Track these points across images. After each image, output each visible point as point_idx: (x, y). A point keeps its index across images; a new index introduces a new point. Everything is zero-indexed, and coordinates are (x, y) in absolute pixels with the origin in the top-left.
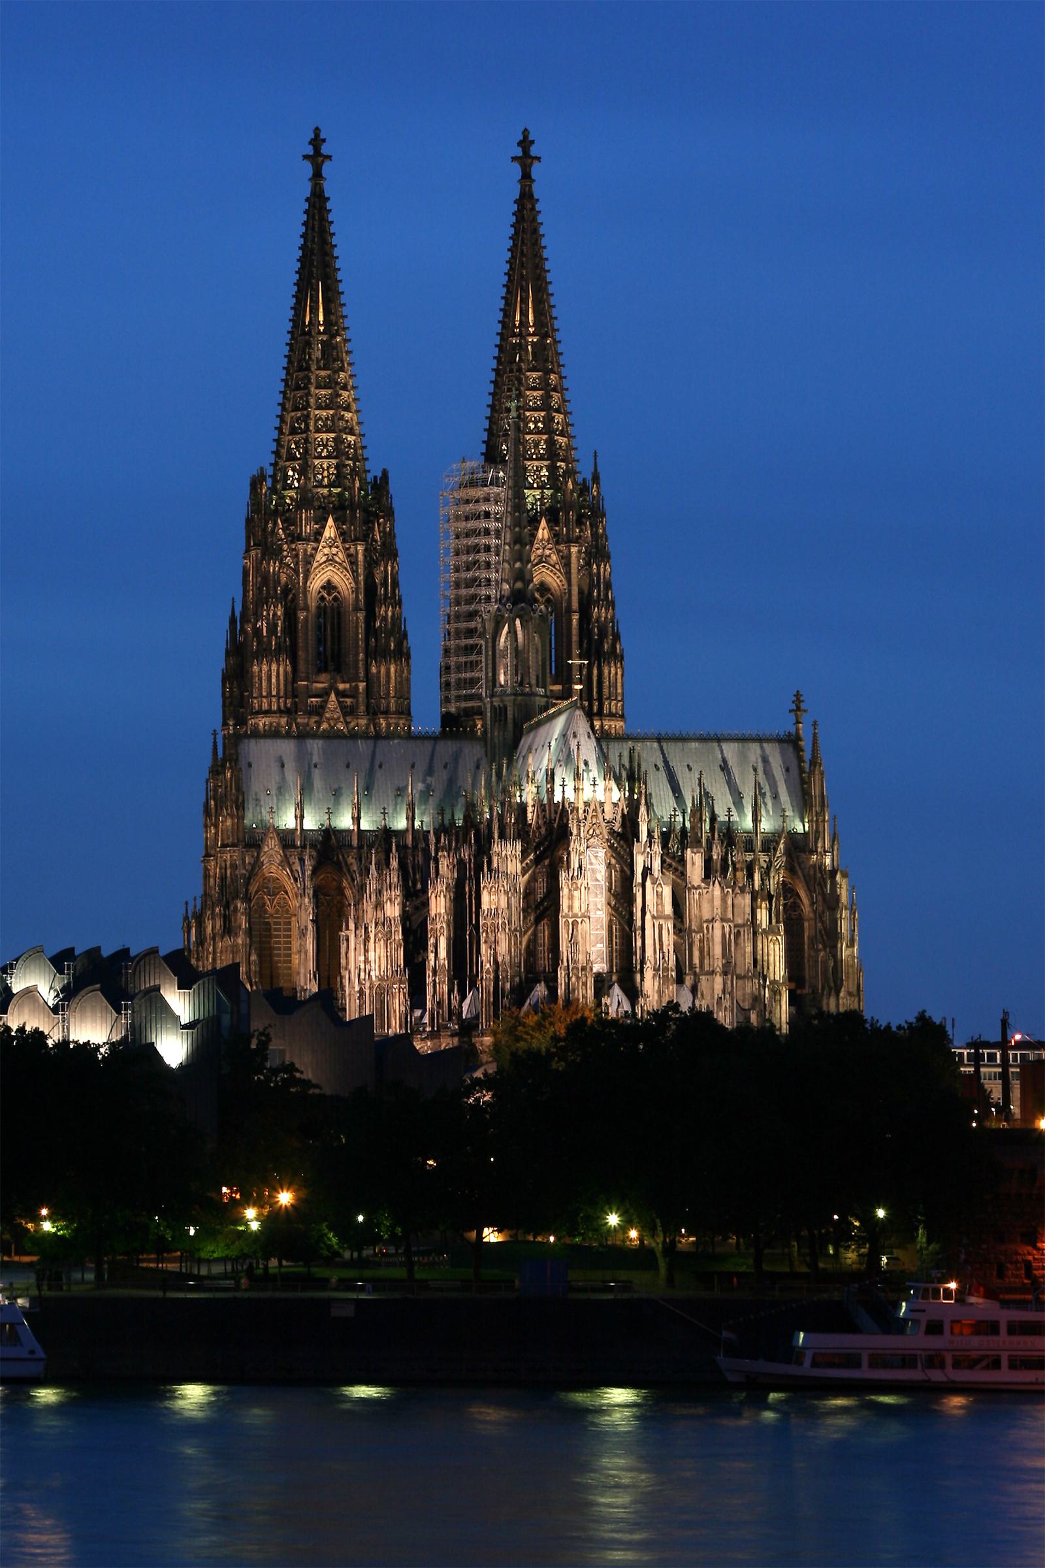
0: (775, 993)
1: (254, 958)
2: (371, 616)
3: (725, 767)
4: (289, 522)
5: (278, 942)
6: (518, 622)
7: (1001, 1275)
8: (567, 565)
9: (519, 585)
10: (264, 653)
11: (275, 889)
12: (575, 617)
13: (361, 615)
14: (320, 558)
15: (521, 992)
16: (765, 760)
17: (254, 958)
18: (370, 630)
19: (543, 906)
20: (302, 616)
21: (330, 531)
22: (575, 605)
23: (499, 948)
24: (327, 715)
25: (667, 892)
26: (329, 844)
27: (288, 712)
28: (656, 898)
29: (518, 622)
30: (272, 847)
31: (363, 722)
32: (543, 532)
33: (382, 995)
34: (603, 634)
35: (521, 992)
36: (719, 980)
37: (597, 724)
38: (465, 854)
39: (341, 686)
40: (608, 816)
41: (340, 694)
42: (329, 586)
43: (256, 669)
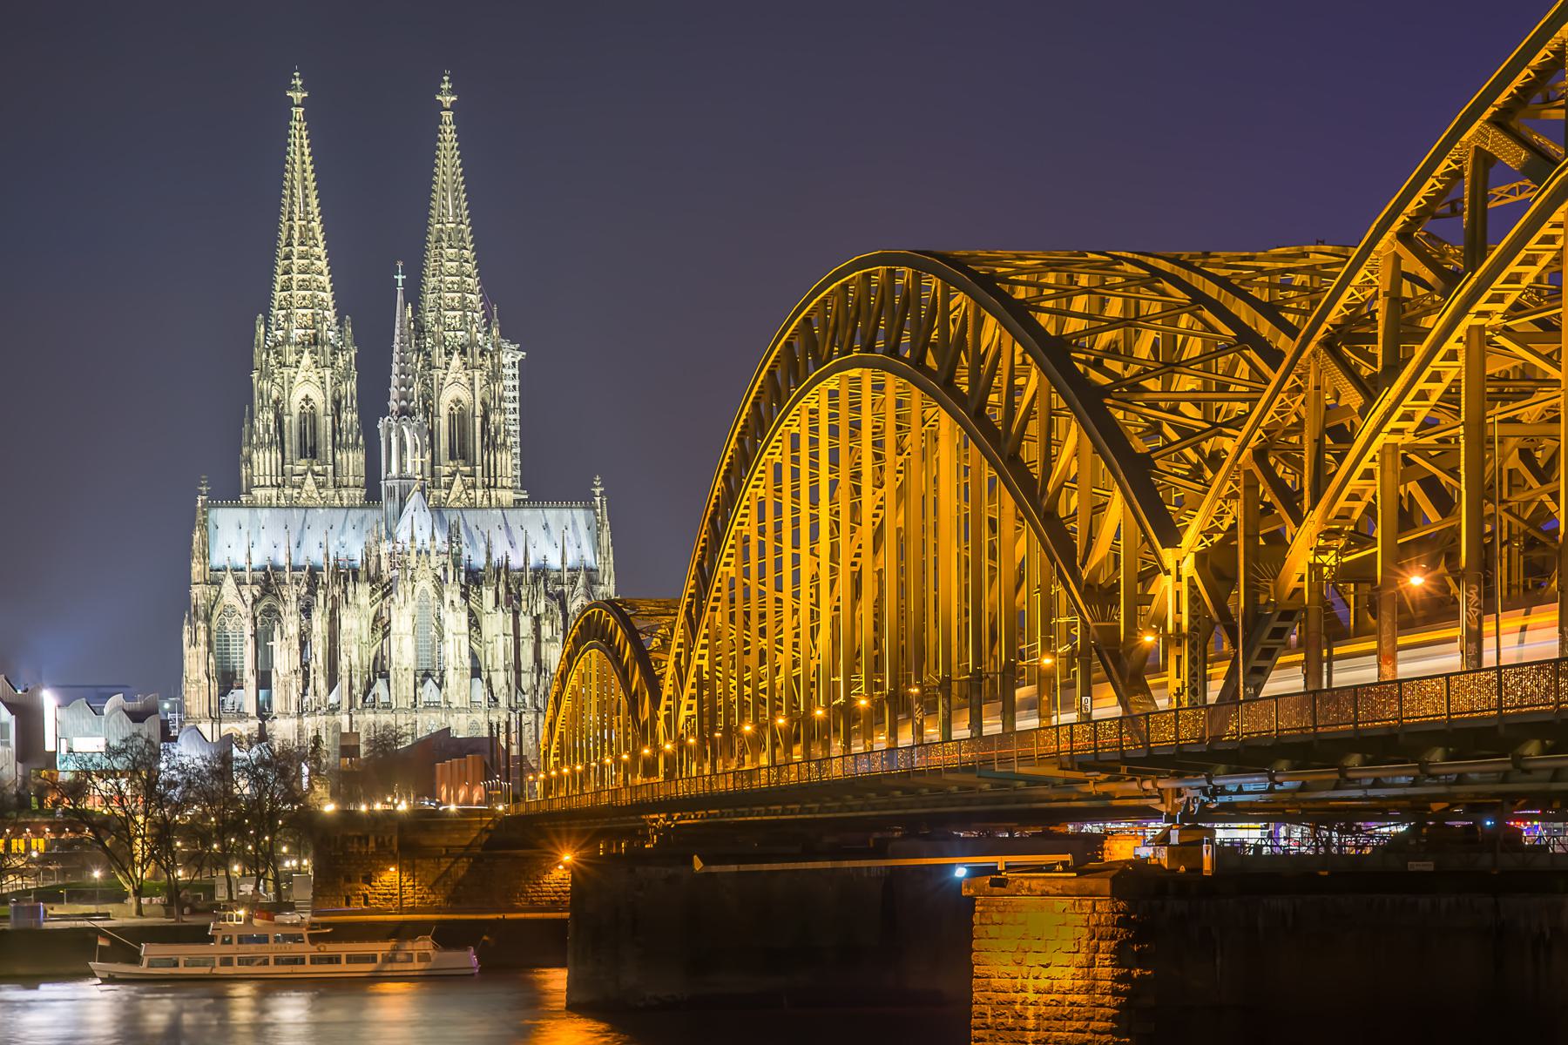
1: (211, 660)
3: (546, 527)
7: (348, 904)
8: (472, 384)
9: (403, 403)
10: (262, 444)
11: (230, 611)
12: (478, 421)
13: (329, 419)
14: (299, 378)
16: (574, 523)
17: (211, 660)
19: (381, 626)
20: (287, 419)
21: (307, 359)
22: (478, 413)
23: (354, 655)
24: (306, 487)
25: (464, 616)
26: (269, 581)
27: (279, 486)
30: (229, 583)
31: (331, 493)
32: (456, 361)
34: (497, 432)
35: (370, 685)
37: (493, 493)
38: (337, 591)
39: (317, 468)
40: (433, 565)
41: (314, 473)
42: (307, 399)
43: (255, 456)
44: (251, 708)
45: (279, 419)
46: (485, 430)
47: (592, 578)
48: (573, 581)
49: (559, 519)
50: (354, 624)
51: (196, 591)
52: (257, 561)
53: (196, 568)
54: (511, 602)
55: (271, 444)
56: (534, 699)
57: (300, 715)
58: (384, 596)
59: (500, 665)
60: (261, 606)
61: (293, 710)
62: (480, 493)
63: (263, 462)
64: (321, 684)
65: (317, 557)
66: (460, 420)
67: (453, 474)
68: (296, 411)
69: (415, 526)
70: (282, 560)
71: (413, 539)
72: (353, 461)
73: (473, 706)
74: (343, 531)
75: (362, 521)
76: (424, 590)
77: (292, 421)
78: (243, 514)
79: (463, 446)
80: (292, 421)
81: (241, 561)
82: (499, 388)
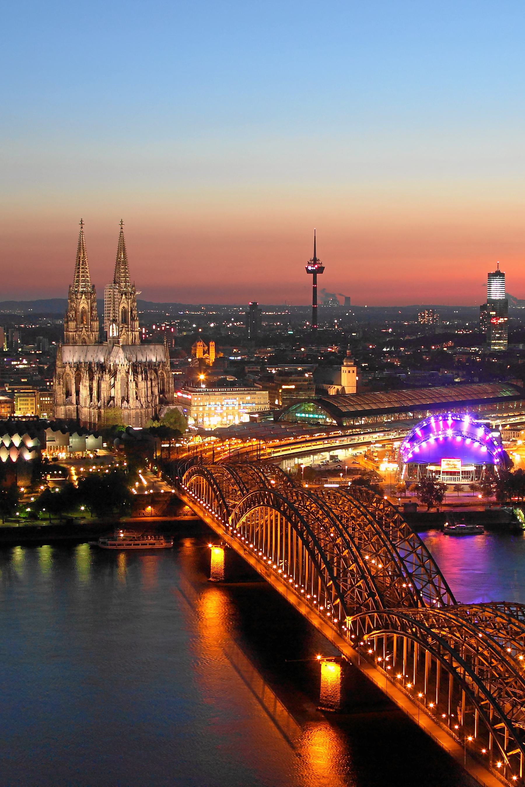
0: (156, 397)
2: (91, 313)
4: (76, 295)
5: (69, 385)
6: (114, 324)
10: (71, 320)
11: (68, 375)
12: (130, 313)
14: (81, 302)
15: (109, 402)
18: (91, 316)
21: (84, 297)
23: (104, 394)
25: (134, 384)
27: (75, 331)
28: (132, 385)
29: (114, 324)
30: (68, 367)
32: (124, 297)
33: (86, 399)
34: (135, 316)
35: (109, 402)
36: (144, 399)
41: (85, 328)
42: (83, 308)
44: (74, 401)
46: (131, 315)
47: (164, 364)
48: (159, 365)
49: (155, 348)
52: (75, 361)
54: (146, 379)
55: (74, 320)
56: (152, 404)
57: (90, 408)
59: (143, 395)
61: (88, 405)
62: (130, 333)
64: (96, 400)
66: (125, 312)
67: (122, 328)
68: (80, 311)
70: (82, 361)
72: (96, 324)
73: (137, 408)
74: (97, 352)
75: (103, 349)
78: (71, 348)
81: (71, 361)
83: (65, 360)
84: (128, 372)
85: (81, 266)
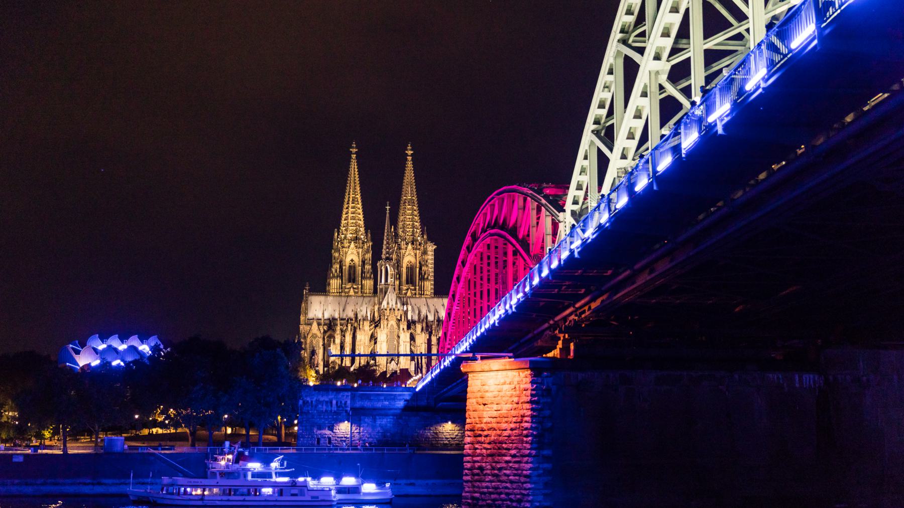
10: (334, 277)
18: (363, 272)
25: (408, 335)
26: (330, 325)
30: (315, 324)
32: (410, 247)
42: (352, 260)
45: (341, 267)
50: (363, 338)
51: (301, 327)
52: (326, 316)
53: (302, 318)
58: (375, 327)
60: (327, 334)
63: (334, 283)
65: (351, 315)
68: (348, 265)
69: (390, 300)
70: (337, 316)
71: (388, 303)
72: (369, 284)
76: (392, 325)
77: (346, 268)
79: (412, 279)
80: (346, 268)
81: (320, 316)
82: (426, 257)
83: (311, 315)
84: (399, 320)
85: (351, 205)
